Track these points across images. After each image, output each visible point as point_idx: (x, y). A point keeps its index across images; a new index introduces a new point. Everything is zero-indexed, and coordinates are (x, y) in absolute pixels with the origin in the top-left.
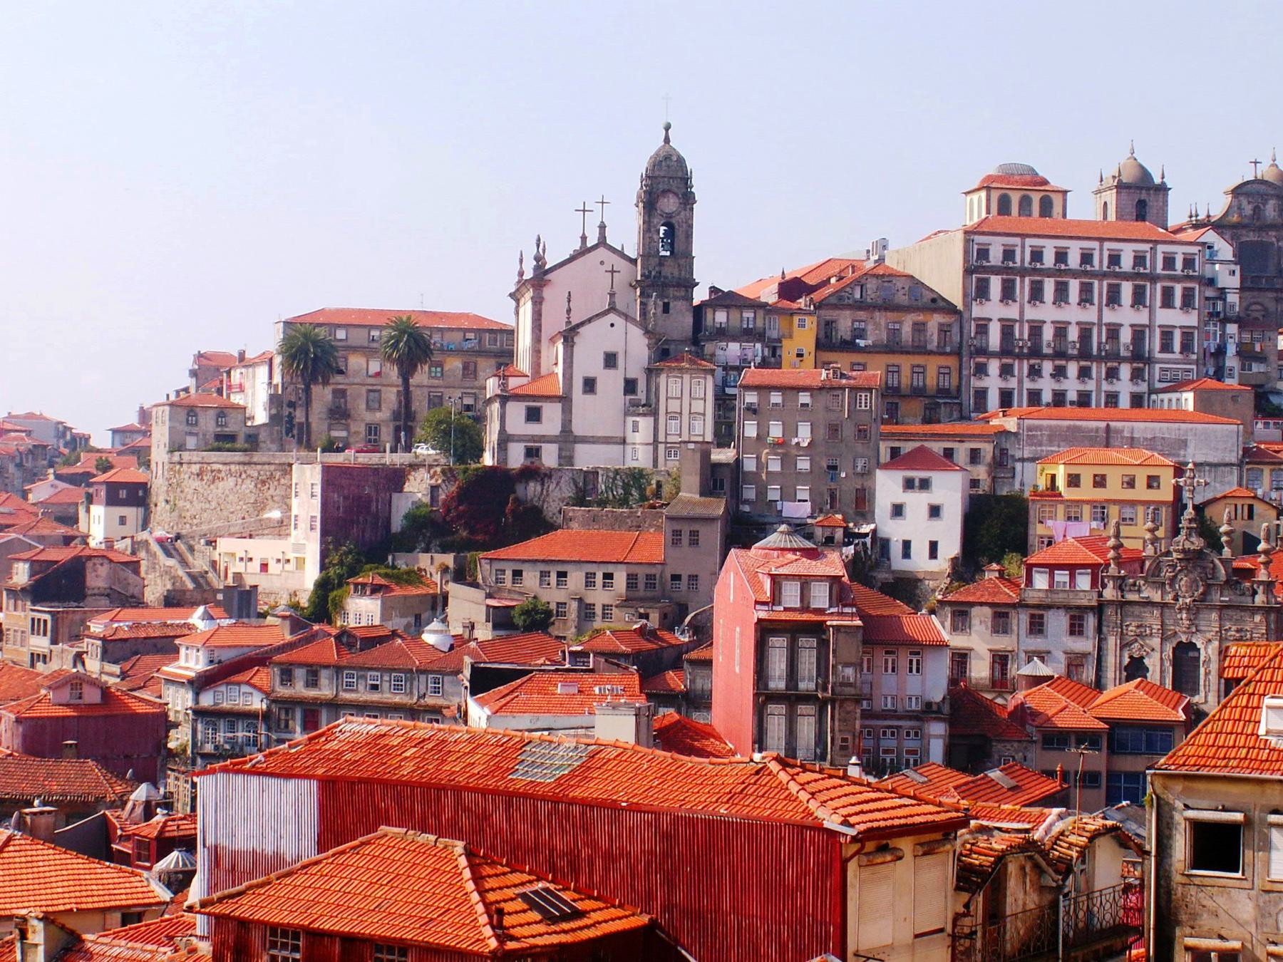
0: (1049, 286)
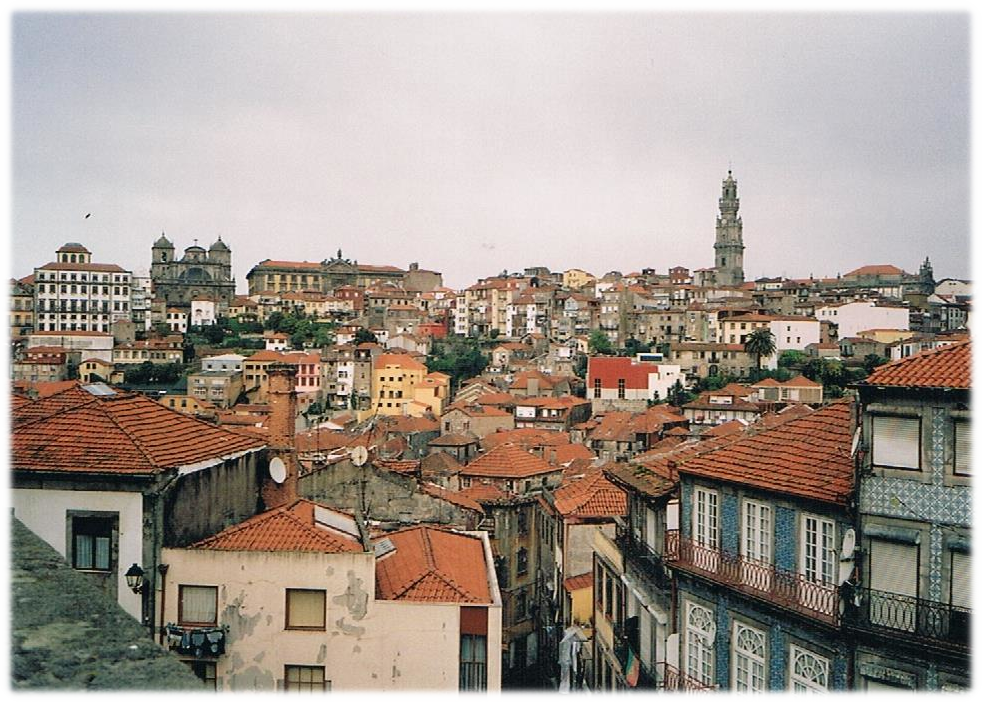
0: (69, 287)
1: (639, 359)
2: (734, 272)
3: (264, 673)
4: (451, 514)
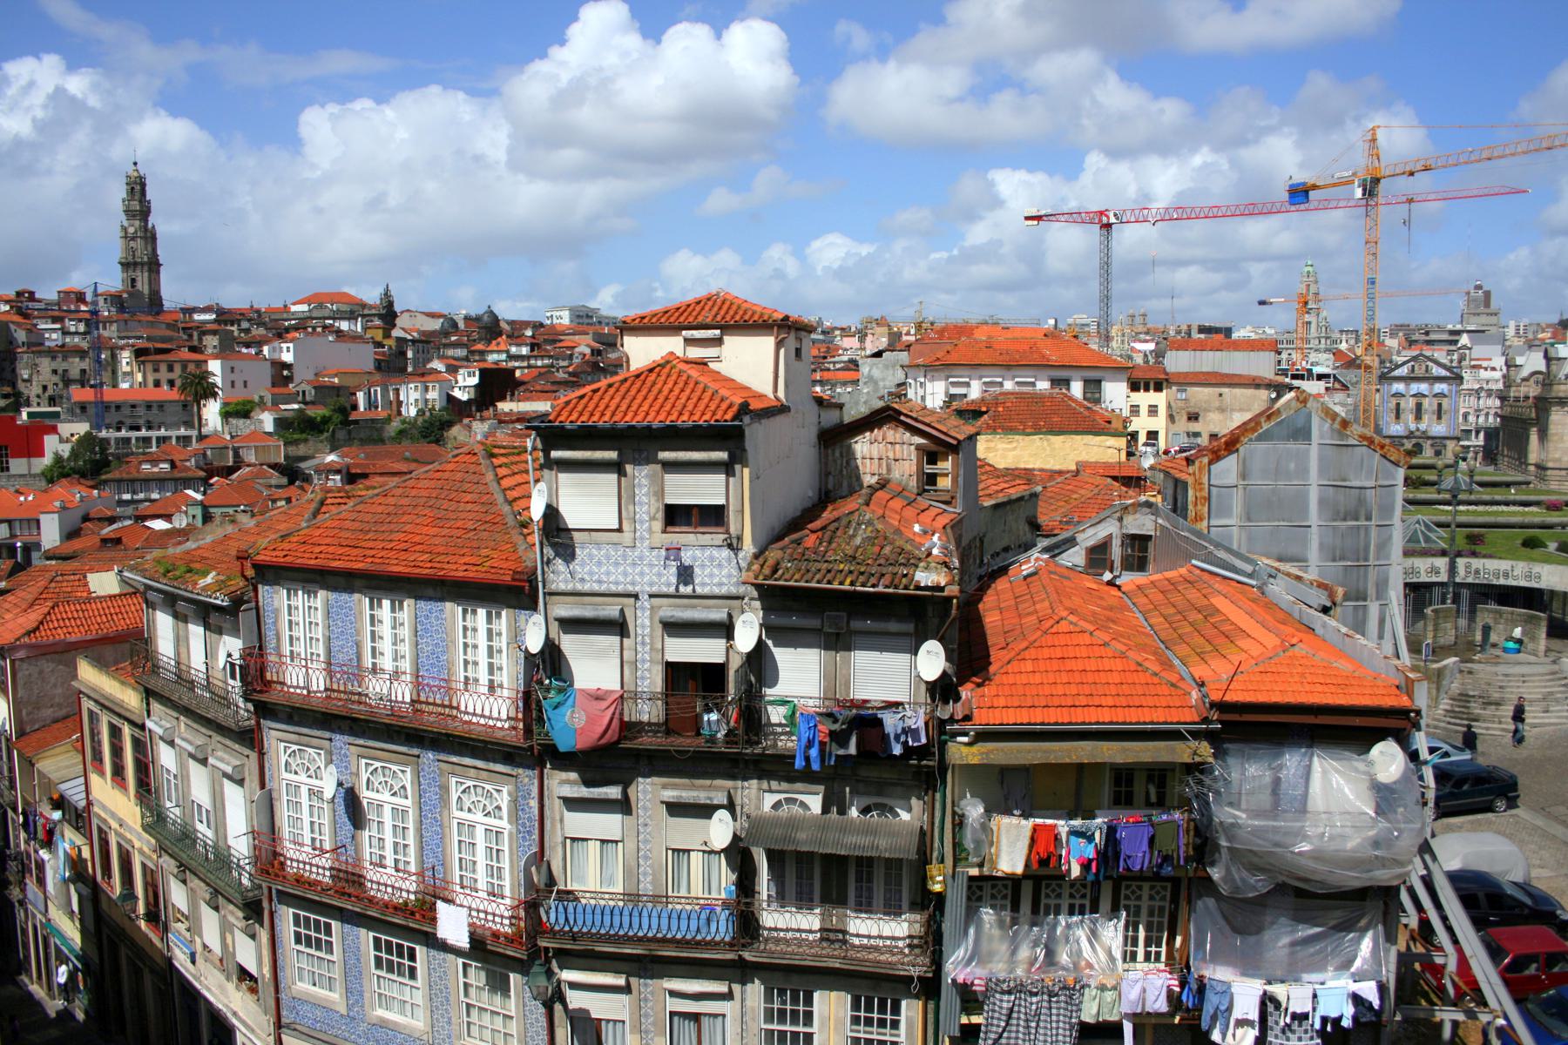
1: (24, 416)
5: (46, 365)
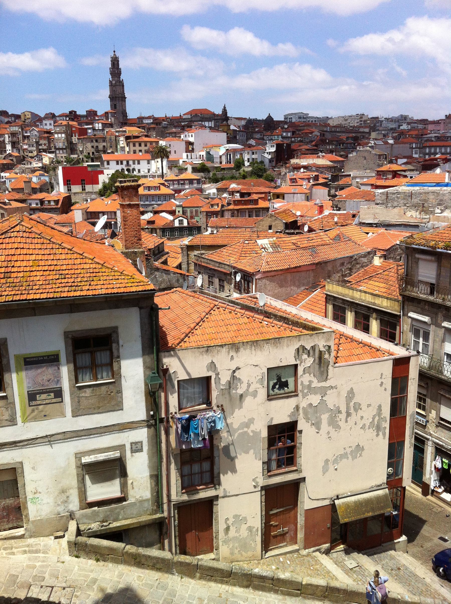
2: (122, 113)
3: (251, 434)
4: (178, 280)
5: (89, 145)
